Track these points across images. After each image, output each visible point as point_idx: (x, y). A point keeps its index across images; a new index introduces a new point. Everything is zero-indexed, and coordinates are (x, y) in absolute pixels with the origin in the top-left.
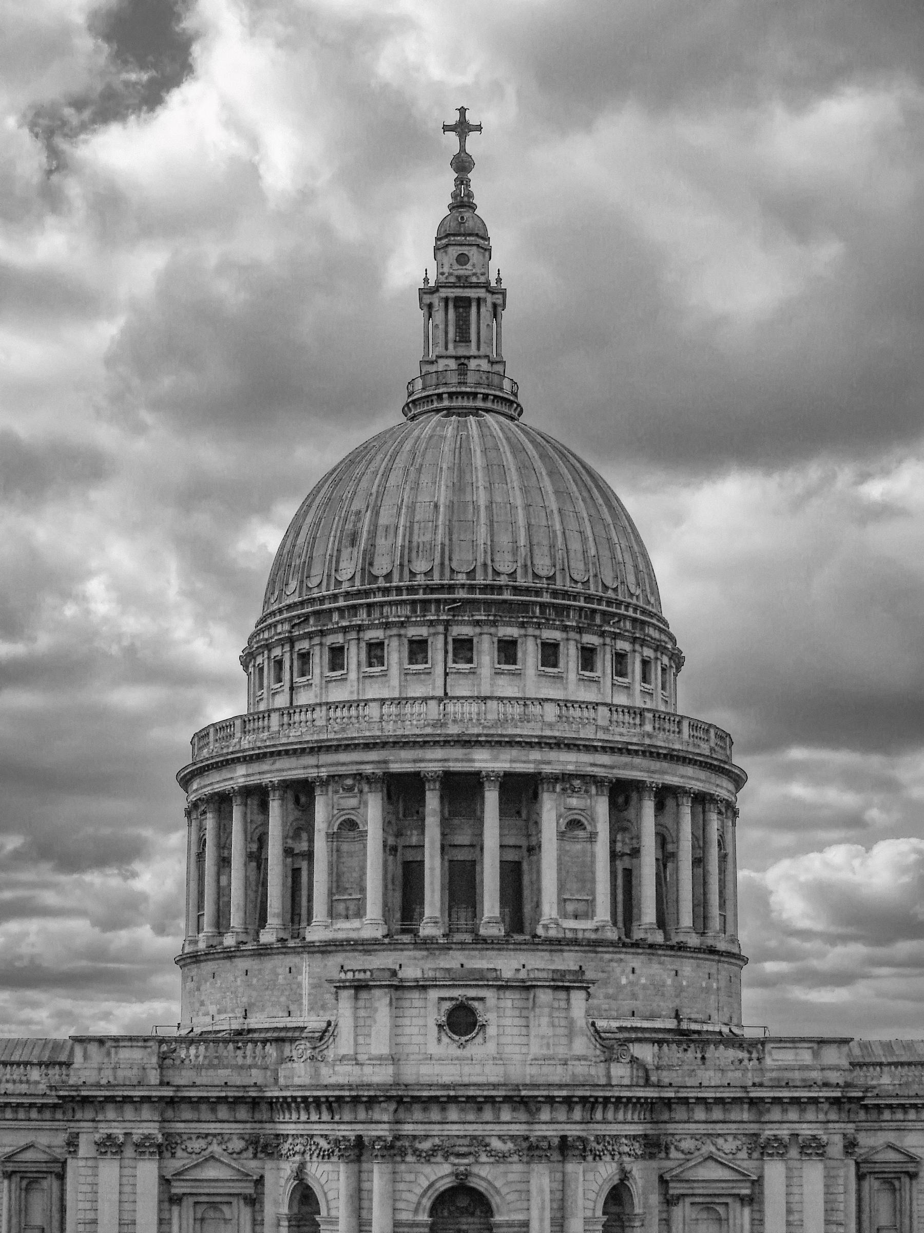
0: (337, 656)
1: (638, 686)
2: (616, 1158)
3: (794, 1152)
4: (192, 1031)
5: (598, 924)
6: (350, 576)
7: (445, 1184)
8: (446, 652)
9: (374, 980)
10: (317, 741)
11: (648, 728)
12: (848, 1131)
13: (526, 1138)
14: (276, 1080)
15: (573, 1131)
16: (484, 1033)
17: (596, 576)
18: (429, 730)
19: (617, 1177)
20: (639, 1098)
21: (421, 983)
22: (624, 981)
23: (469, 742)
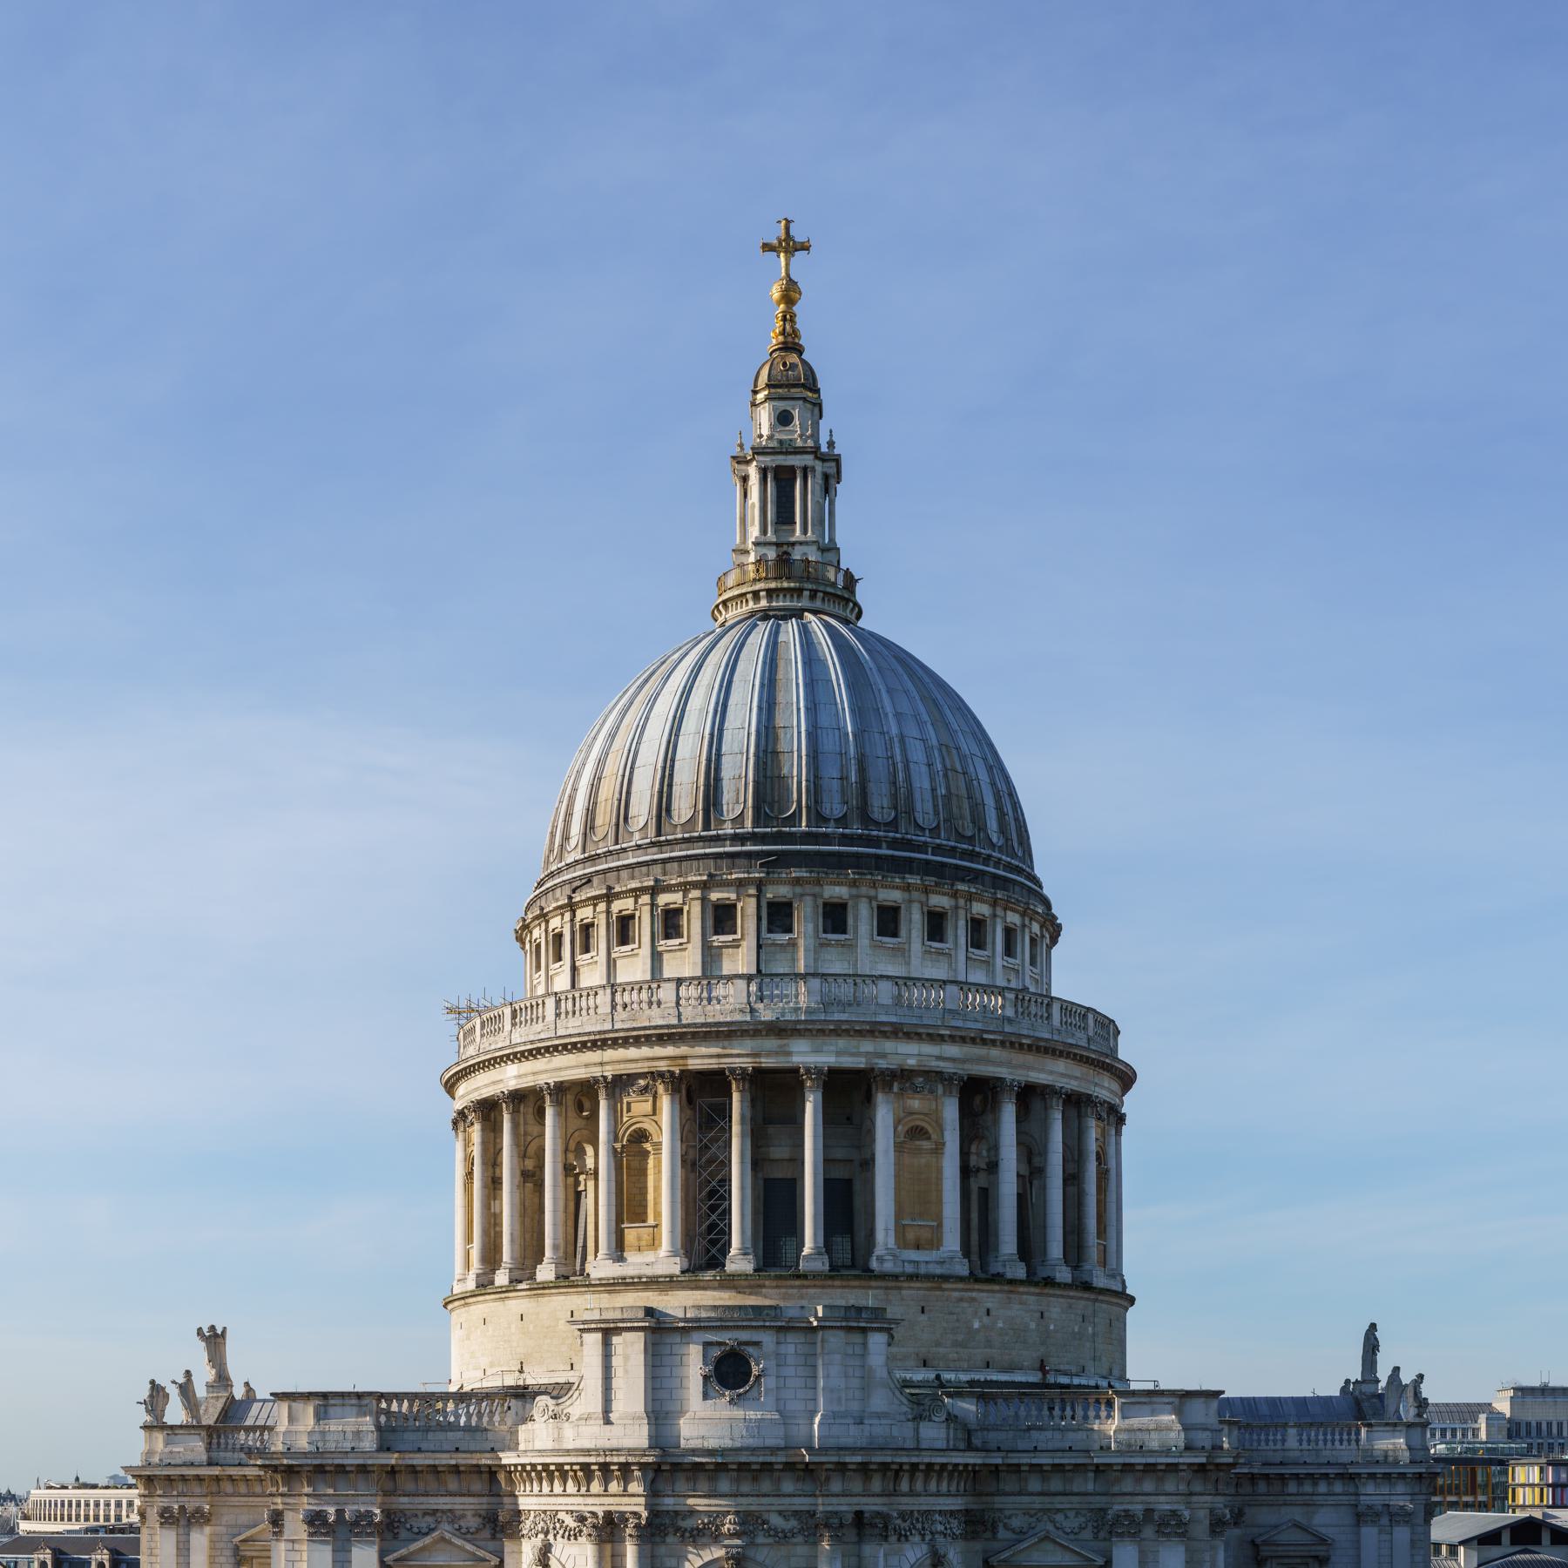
2: (928, 1538)
3: (1149, 1532)
5: (945, 1255)
8: (759, 919)
10: (600, 1033)
13: (812, 1514)
15: (871, 1505)
20: (956, 1465)
22: (976, 1325)
23: (784, 1030)
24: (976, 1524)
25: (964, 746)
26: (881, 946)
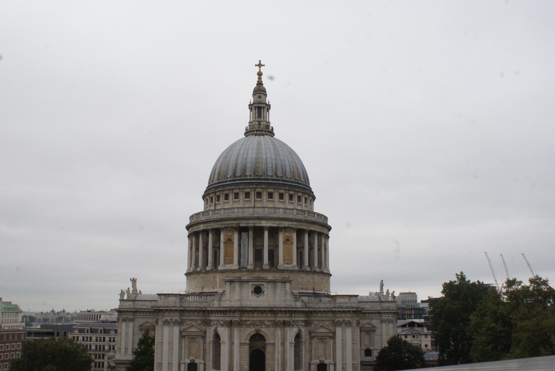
0: (227, 197)
1: (304, 205)
2: (298, 326)
3: (344, 325)
4: (189, 293)
6: (230, 176)
7: (253, 333)
8: (255, 195)
9: (235, 280)
11: (306, 215)
12: (358, 319)
13: (274, 321)
14: (210, 305)
15: (287, 319)
16: (264, 294)
17: (293, 176)
18: (250, 216)
19: (298, 331)
20: (304, 311)
21: (247, 281)
24: (307, 323)
25: (296, 161)
26: (279, 202)
